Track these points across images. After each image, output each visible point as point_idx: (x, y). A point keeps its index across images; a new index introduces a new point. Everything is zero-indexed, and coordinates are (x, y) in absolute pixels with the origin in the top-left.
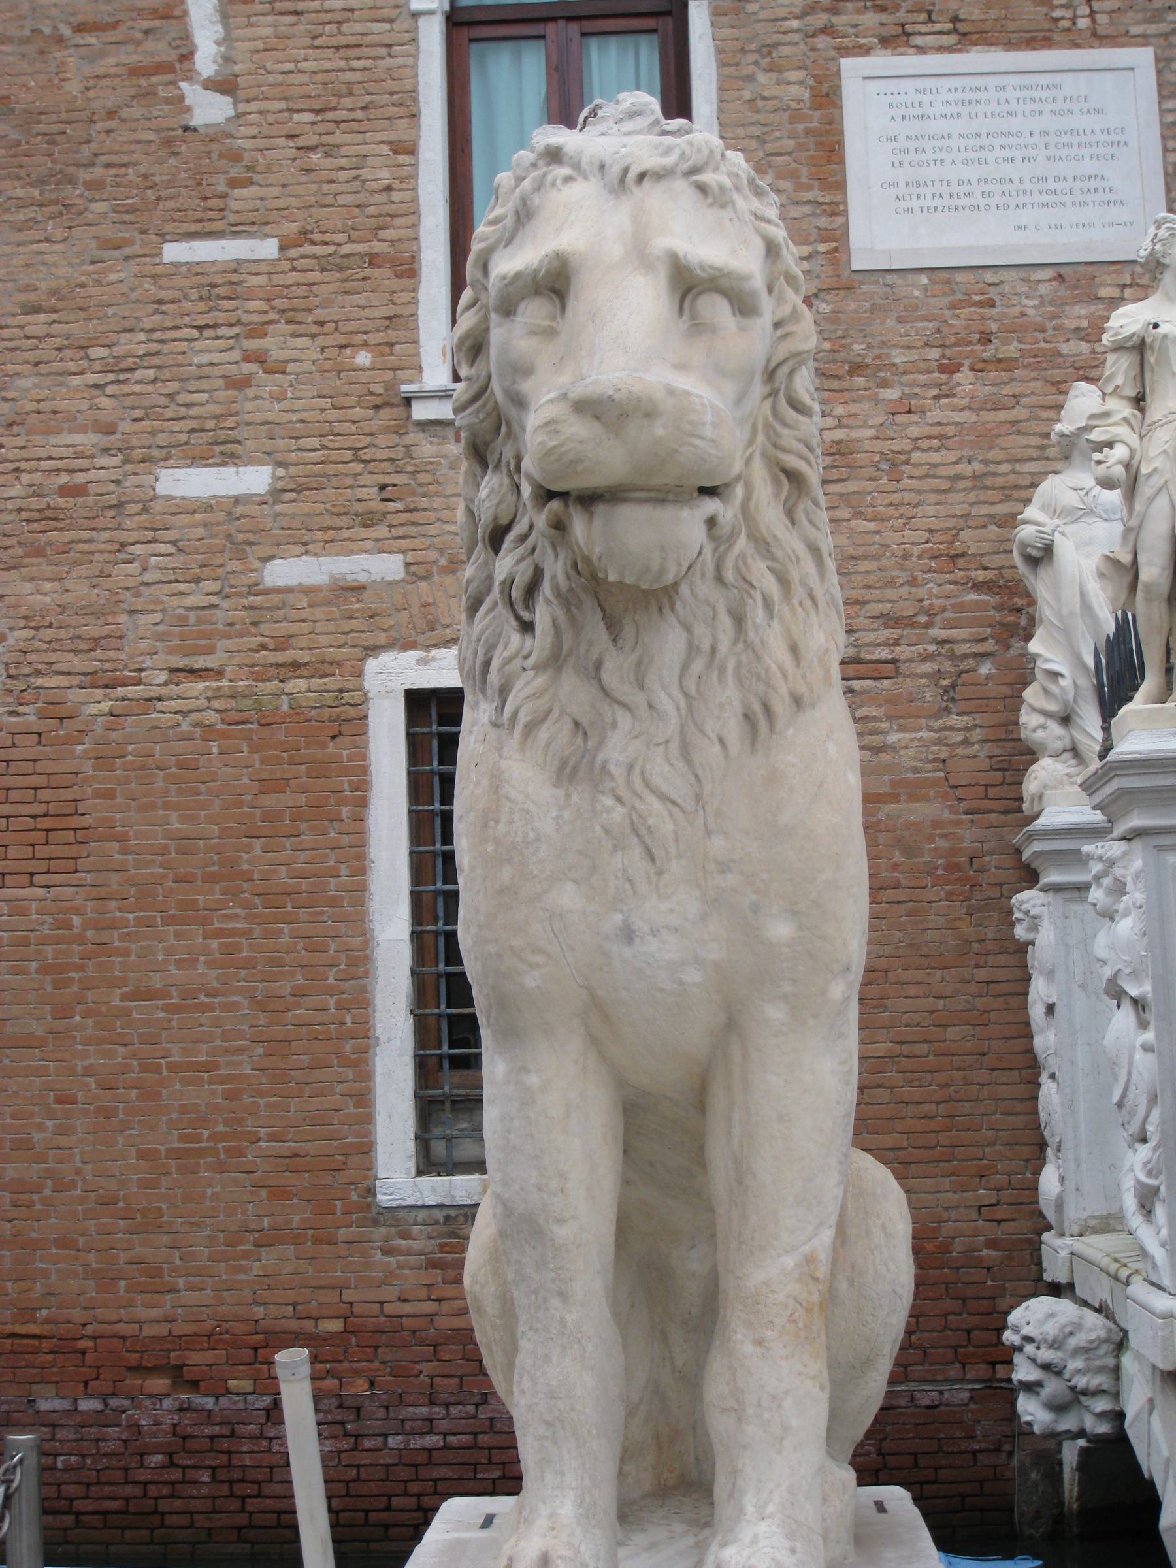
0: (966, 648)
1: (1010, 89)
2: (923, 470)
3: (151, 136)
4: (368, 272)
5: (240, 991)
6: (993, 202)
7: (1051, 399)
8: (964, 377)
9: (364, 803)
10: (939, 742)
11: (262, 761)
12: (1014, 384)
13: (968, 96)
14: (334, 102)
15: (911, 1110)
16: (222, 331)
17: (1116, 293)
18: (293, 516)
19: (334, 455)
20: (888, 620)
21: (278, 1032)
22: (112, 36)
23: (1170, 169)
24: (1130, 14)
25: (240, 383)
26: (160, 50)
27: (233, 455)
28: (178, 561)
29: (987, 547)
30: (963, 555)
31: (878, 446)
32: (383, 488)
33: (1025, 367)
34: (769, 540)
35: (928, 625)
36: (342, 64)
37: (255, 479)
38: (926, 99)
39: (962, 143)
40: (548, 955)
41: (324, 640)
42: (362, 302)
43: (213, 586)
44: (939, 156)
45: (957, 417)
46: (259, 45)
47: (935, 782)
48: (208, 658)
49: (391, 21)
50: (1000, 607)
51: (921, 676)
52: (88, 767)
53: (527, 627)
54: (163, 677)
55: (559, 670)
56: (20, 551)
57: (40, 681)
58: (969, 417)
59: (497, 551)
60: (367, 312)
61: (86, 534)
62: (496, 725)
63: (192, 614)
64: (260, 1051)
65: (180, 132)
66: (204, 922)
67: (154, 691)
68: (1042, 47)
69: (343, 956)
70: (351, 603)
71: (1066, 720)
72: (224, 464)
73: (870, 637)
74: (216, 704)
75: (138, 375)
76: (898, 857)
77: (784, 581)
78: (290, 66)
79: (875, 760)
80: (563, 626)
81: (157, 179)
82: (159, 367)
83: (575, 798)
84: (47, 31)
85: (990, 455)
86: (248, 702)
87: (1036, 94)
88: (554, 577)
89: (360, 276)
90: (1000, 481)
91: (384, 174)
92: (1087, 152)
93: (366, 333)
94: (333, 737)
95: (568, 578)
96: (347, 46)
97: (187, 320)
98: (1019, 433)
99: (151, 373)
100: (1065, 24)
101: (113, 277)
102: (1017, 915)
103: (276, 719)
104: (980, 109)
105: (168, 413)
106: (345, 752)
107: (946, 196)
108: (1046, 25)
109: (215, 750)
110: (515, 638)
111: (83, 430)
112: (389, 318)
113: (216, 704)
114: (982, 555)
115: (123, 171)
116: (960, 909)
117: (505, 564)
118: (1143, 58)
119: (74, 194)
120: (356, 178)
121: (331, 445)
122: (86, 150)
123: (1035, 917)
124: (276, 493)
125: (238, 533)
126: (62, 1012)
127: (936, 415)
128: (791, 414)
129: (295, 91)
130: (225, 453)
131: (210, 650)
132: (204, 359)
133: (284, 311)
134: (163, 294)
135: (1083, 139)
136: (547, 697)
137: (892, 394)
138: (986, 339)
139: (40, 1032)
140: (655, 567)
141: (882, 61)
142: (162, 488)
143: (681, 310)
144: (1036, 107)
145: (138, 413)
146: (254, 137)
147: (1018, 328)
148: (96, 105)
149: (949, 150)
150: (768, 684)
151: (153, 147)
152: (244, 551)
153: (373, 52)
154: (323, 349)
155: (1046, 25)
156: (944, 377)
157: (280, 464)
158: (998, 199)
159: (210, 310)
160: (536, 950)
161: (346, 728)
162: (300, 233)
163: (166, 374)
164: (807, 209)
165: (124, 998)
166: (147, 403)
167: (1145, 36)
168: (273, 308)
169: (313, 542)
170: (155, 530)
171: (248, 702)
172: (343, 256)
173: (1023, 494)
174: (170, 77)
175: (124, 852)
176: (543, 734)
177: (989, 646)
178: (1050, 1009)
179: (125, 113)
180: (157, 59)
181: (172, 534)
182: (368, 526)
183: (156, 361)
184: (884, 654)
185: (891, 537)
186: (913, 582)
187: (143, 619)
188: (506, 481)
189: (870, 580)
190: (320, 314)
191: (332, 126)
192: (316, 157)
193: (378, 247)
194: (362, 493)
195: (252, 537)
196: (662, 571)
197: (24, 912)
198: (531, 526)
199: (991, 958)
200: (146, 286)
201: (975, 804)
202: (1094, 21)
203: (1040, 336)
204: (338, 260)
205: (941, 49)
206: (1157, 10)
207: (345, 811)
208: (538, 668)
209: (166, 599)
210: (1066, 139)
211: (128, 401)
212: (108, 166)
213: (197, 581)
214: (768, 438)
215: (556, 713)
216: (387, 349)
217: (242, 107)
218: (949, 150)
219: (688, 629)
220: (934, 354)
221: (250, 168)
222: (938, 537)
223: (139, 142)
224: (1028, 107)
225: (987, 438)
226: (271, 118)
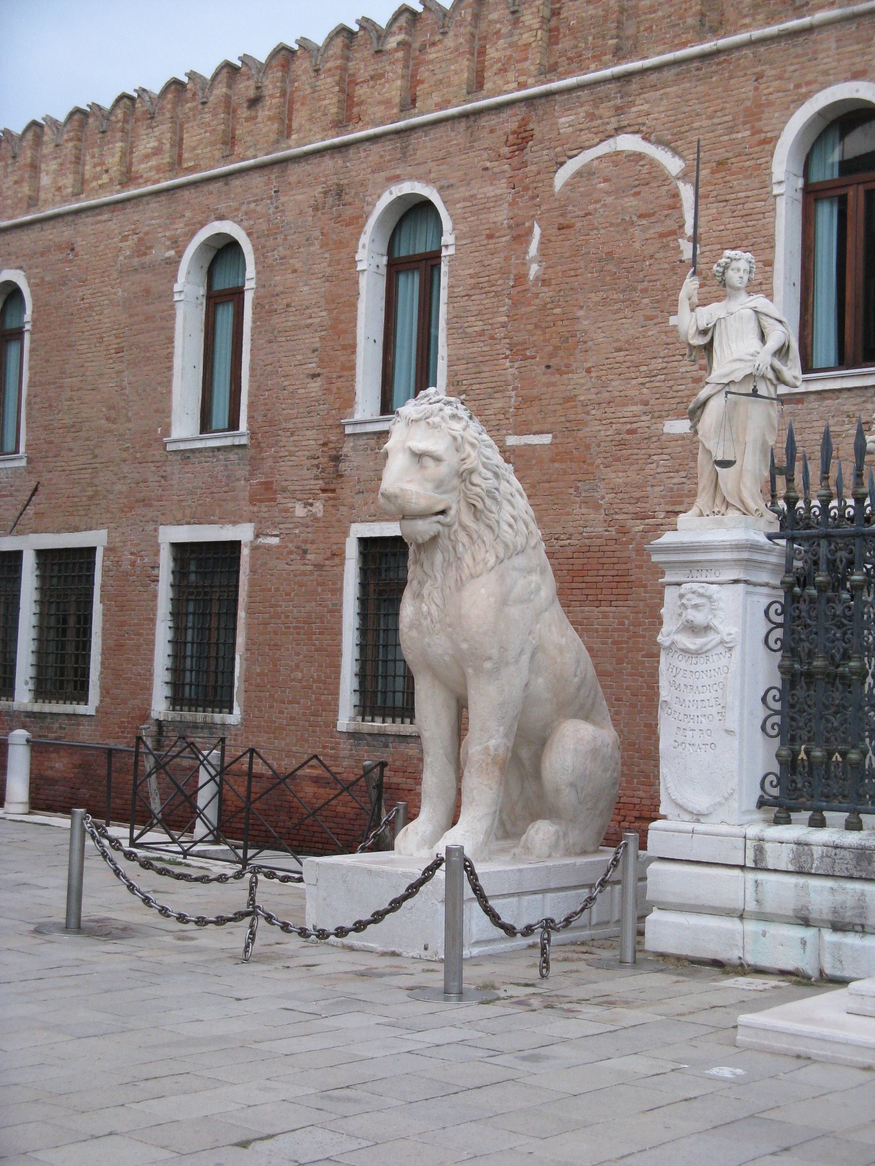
3: (666, 266)
14: (740, 243)
22: (653, 219)
26: (670, 224)
43: (683, 474)
46: (710, 218)
49: (765, 201)
52: (633, 555)
54: (662, 515)
56: (611, 459)
57: (617, 517)
61: (636, 451)
67: (660, 521)
78: (722, 227)
84: (628, 219)
101: (650, 333)
111: (636, 404)
119: (636, 295)
122: (641, 275)
126: (620, 661)
129: (725, 239)
139: (611, 670)
142: (666, 430)
145: (657, 396)
148: (645, 253)
153: (755, 217)
163: (669, 377)
165: (643, 656)
175: (645, 592)
183: (665, 371)
187: (657, 489)
197: (607, 617)
211: (654, 390)
212: (650, 281)
213: (677, 471)
226: (714, 253)
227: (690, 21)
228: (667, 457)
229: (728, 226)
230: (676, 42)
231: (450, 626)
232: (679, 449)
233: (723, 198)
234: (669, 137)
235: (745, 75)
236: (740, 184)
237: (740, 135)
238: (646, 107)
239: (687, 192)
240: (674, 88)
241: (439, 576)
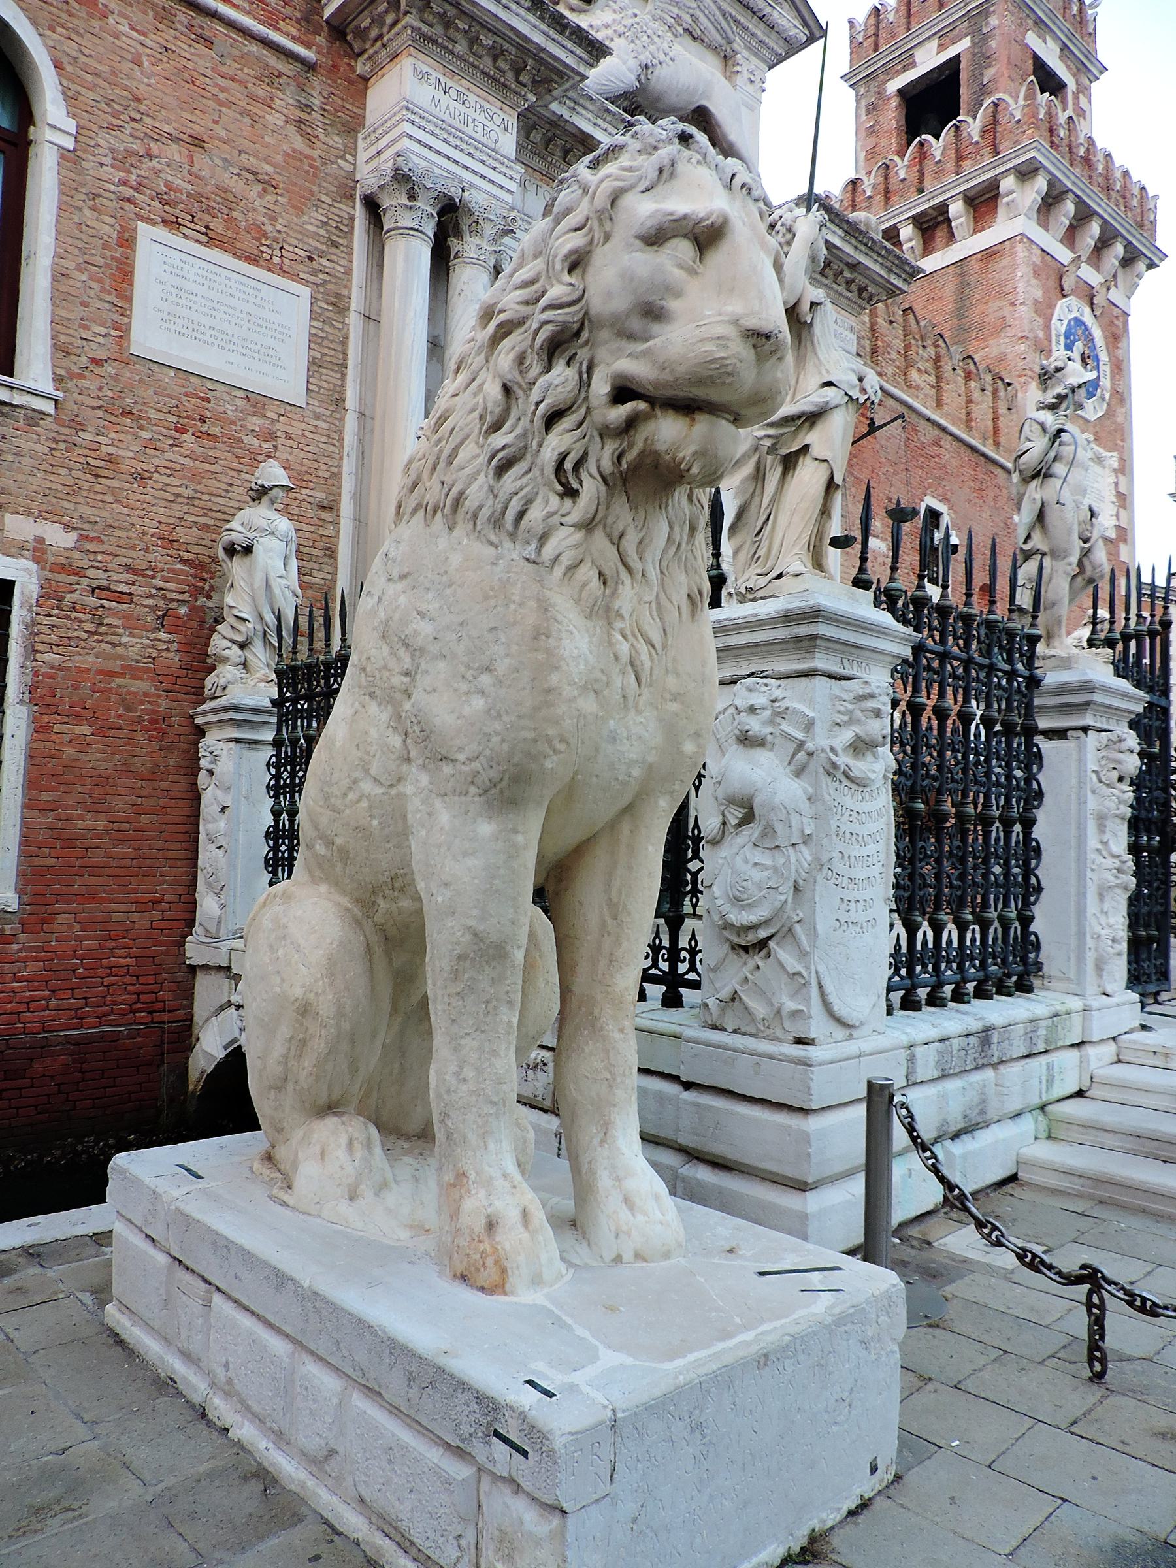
0: (173, 595)
2: (159, 486)
8: (188, 437)
10: (152, 647)
13: (209, 275)
15: (115, 863)
17: (275, 417)
20: (129, 569)
29: (191, 540)
30: (177, 541)
31: (134, 463)
33: (224, 443)
35: (153, 577)
38: (186, 267)
47: (147, 670)
50: (195, 576)
51: (146, 606)
71: (242, 646)
73: (116, 577)
76: (121, 711)
79: (113, 651)
85: (199, 488)
87: (248, 290)
92: (270, 333)
98: (215, 479)
108: (256, 252)
116: (156, 745)
127: (169, 455)
137: (146, 435)
141: (161, 233)
144: (247, 297)
147: (220, 419)
155: (256, 252)
156: (177, 434)
160: (562, 740)
164: (107, 306)
177: (186, 597)
184: (124, 588)
185: (135, 520)
186: (146, 550)
189: (120, 543)
201: (170, 687)
208: (577, 526)
210: (260, 322)
220: (173, 419)
222: (163, 527)
224: (242, 296)
225: (197, 477)
231: (675, 697)
241: (653, 574)
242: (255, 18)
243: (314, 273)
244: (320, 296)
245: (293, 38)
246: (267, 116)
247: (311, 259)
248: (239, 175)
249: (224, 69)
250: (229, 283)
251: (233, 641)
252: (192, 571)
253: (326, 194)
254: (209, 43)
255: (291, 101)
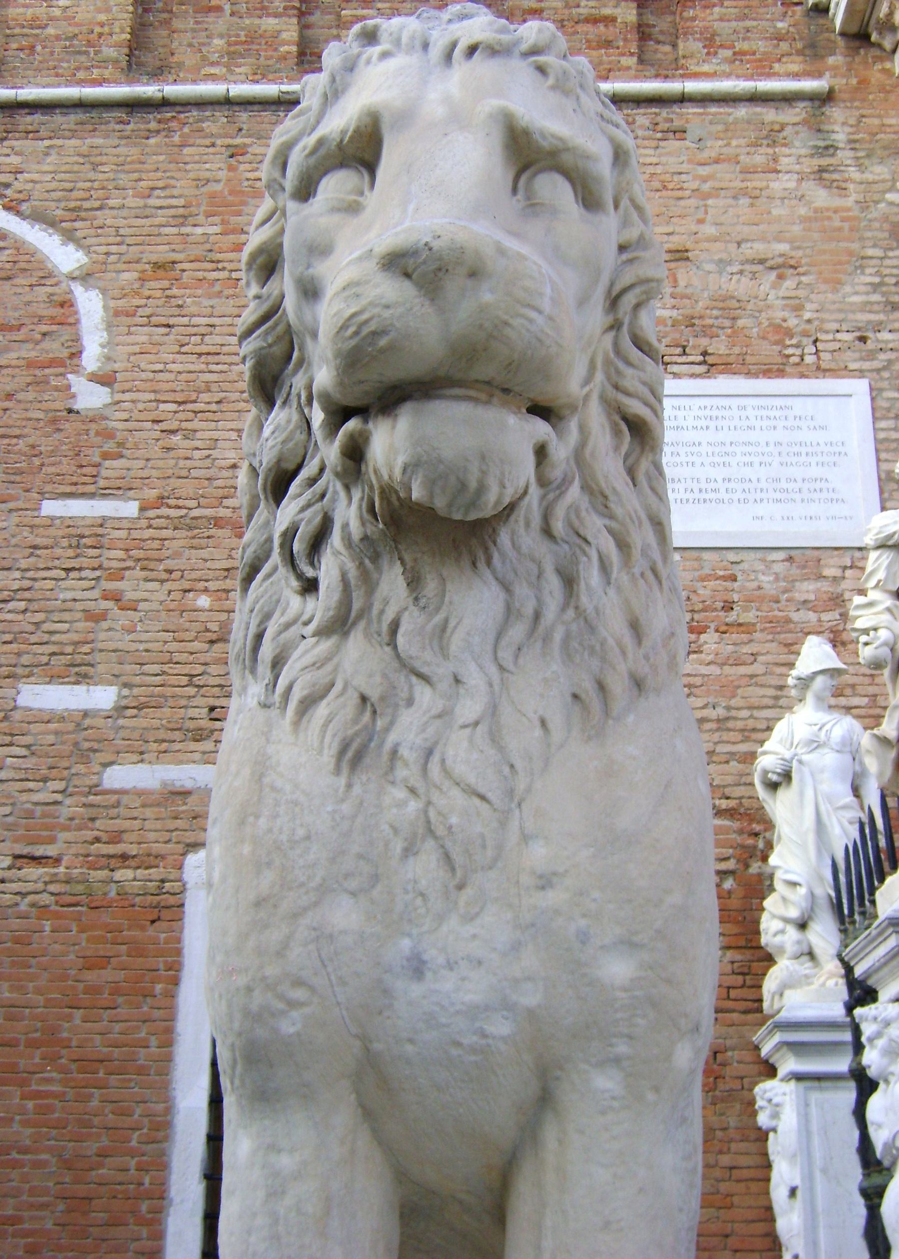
1: (749, 409)
3: (41, 415)
4: (212, 532)
5: (50, 1150)
6: (735, 497)
7: (783, 658)
8: (709, 638)
9: (176, 982)
11: (88, 941)
12: (752, 644)
13: (715, 413)
16: (84, 574)
17: (837, 572)
18: (134, 729)
19: (173, 680)
21: (81, 1190)
23: (883, 476)
24: (849, 353)
25: (99, 617)
26: (55, 348)
27: (86, 676)
28: (29, 763)
29: (729, 780)
32: (212, 709)
33: (762, 631)
34: (608, 492)
36: (203, 367)
37: (103, 697)
39: (710, 450)
40: (312, 989)
41: (152, 836)
42: (206, 556)
44: (690, 459)
45: (704, 670)
46: (137, 349)
48: (49, 847)
50: (741, 832)
53: (310, 586)
55: (346, 634)
58: (714, 670)
59: (278, 502)
60: (209, 564)
62: (265, 706)
63: (39, 808)
64: (61, 1207)
65: (65, 413)
66: (23, 1083)
68: (777, 377)
69: (146, 1120)
70: (178, 805)
72: (77, 683)
74: (52, 888)
75: (11, 605)
77: (623, 545)
78: (160, 367)
80: (353, 582)
81: (42, 449)
82: (29, 600)
83: (357, 789)
85: (733, 703)
86: (80, 888)
87: (772, 414)
88: (345, 526)
89: (206, 535)
90: (739, 724)
91: (232, 454)
92: (813, 460)
93: (207, 581)
94: (153, 922)
95: (363, 524)
96: (208, 354)
97: (57, 563)
98: (757, 685)
99: (22, 605)
100: (796, 359)
102: (760, 1103)
103: (104, 903)
104: (725, 423)
105: (34, 639)
106: (163, 936)
107: (696, 491)
108: (779, 360)
109: (48, 928)
110: (295, 602)
112: (227, 570)
113: (52, 888)
114: (724, 786)
115: (15, 441)
117: (289, 511)
118: (860, 387)
120: (208, 457)
121: (171, 671)
123: (777, 1105)
124: (120, 709)
125: (84, 742)
128: (635, 354)
130: (80, 673)
131: (52, 840)
132: (69, 595)
133: (139, 560)
134: (39, 541)
135: (810, 450)
136: (329, 667)
138: (728, 607)
140: (473, 485)
142: (22, 701)
143: (515, 190)
144: (772, 423)
145: (8, 637)
146: (126, 421)
147: (755, 598)
149: (699, 454)
150: (604, 659)
151: (42, 424)
152: (88, 756)
154: (170, 592)
155: (779, 360)
157: (125, 685)
158: (739, 495)
159: (77, 556)
160: (299, 983)
161: (165, 914)
162: (159, 498)
166: (16, 629)
167: (861, 371)
168: (130, 557)
169: (150, 752)
170: (12, 735)
171: (80, 888)
172: (192, 518)
173: (759, 736)
174: (61, 370)
176: (322, 710)
178: (793, 1192)
179: (20, 396)
180: (51, 355)
181: (28, 740)
182: (198, 741)
188: (295, 417)
190: (170, 564)
191: (191, 415)
192: (176, 439)
193: (222, 512)
194: (192, 712)
195: (96, 746)
196: (482, 489)
198: (322, 470)
199: (733, 1146)
200: (25, 534)
202: (819, 358)
203: (775, 606)
204: (188, 521)
205: (693, 376)
206: (871, 351)
207: (159, 988)
208: (323, 632)
209: (17, 794)
210: (796, 449)
213: (45, 780)
214: (609, 378)
215: (339, 686)
216: (224, 595)
217: (119, 397)
218: (699, 454)
219: (507, 588)
221: (120, 445)
223: (30, 419)
224: (765, 423)
225: (730, 689)
226: (141, 406)
227: (110, 52)
228: (23, 752)
229: (171, 367)
230: (81, 75)
232: (51, 738)
233: (163, 320)
234: (59, 212)
235: (213, 145)
236: (199, 304)
237: (199, 230)
238: (15, 160)
239: (90, 305)
240: (73, 142)
242: (738, 77)
243: (871, 356)
244: (885, 384)
245: (796, 76)
246: (772, 185)
247: (863, 339)
248: (741, 272)
249: (705, 155)
250: (743, 414)
251: (786, 920)
252: (736, 825)
253: (875, 246)
254: (680, 133)
255: (803, 151)
